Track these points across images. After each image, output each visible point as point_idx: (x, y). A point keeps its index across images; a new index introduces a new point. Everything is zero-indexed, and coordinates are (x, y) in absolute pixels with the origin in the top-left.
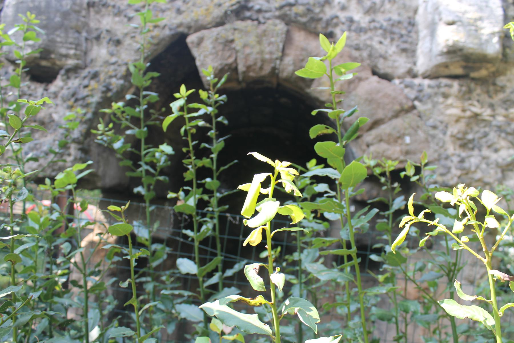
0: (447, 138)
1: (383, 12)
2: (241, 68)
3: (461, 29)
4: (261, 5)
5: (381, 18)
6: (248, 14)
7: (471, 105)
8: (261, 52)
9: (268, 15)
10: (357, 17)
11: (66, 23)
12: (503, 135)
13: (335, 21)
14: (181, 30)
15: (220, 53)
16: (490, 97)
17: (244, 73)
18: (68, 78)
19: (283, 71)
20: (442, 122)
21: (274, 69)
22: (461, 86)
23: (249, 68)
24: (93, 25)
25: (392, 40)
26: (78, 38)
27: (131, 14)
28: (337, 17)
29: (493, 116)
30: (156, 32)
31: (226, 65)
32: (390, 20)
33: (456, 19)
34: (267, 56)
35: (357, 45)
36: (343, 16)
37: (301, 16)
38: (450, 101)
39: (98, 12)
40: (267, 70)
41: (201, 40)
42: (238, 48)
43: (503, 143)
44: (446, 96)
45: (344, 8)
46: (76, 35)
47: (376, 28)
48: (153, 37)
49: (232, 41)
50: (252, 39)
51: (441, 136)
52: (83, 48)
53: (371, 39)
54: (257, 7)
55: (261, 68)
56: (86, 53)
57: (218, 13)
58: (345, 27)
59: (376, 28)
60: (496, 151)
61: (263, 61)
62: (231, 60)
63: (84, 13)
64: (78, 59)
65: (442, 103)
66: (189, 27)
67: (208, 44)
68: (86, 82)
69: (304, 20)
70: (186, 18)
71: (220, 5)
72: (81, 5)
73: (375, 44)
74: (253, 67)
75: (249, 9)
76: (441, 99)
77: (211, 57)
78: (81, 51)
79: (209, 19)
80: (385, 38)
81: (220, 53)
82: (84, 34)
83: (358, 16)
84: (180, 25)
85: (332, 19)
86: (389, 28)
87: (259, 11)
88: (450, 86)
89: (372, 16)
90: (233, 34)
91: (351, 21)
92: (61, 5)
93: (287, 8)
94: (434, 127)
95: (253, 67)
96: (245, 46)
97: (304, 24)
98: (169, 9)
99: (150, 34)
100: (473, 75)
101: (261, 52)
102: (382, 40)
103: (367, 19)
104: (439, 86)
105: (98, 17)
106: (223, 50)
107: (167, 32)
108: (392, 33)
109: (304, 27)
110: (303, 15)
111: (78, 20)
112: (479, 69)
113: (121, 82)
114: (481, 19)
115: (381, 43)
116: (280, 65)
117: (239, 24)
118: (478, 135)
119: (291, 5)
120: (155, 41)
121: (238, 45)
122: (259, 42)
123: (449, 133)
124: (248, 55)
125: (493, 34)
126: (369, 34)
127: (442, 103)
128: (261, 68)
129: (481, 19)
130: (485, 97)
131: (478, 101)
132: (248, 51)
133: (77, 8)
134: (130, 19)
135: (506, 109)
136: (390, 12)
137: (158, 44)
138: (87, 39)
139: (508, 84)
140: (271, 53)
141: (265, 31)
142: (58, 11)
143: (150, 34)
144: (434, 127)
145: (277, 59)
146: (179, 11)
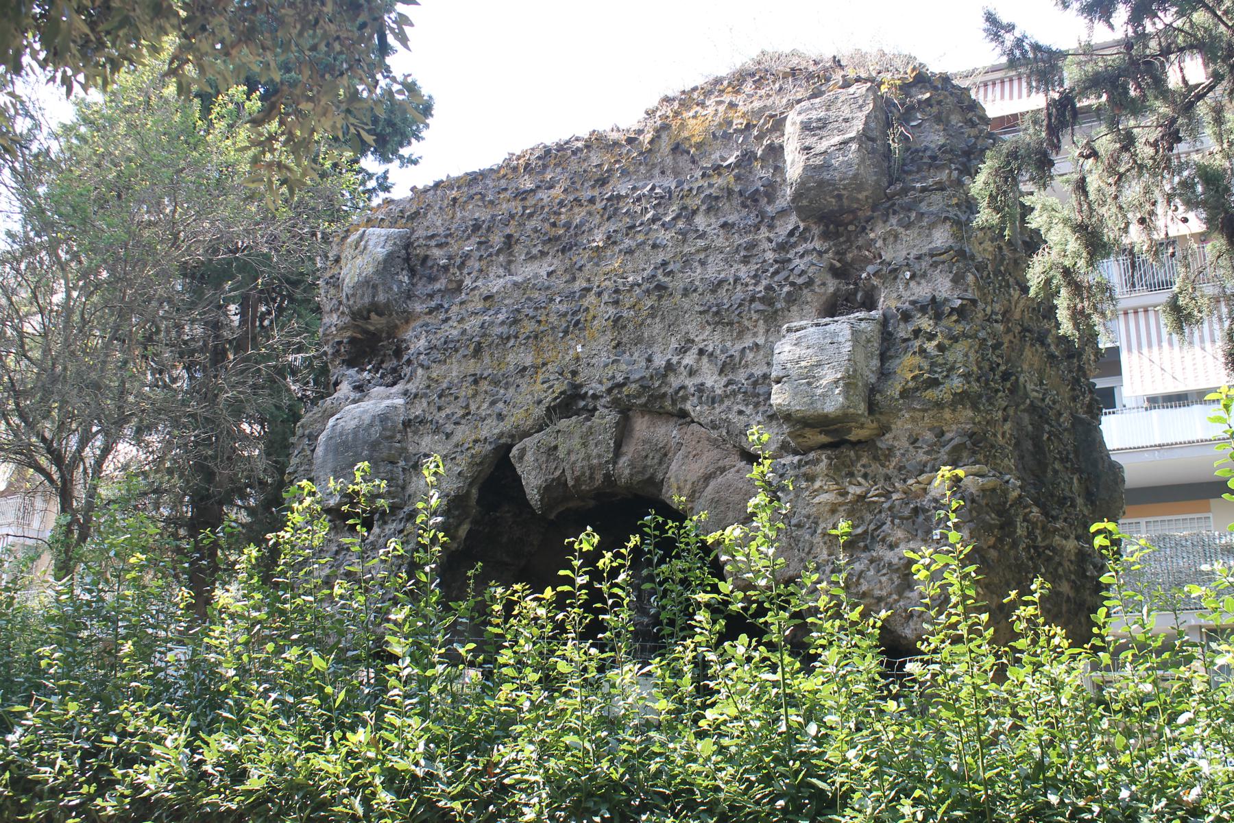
0: (817, 539)
1: (746, 366)
2: (571, 483)
3: (786, 386)
4: (595, 389)
5: (741, 376)
6: (582, 404)
7: (850, 483)
8: (588, 457)
9: (603, 401)
10: (709, 383)
11: (375, 454)
12: (897, 521)
13: (681, 393)
14: (503, 441)
15: (544, 466)
16: (883, 466)
18: (385, 523)
19: (620, 476)
20: (808, 517)
21: (607, 476)
22: (829, 458)
23: (577, 479)
24: (411, 449)
25: (757, 405)
26: (391, 471)
27: (449, 428)
28: (683, 387)
29: (887, 494)
30: (478, 448)
31: (553, 480)
32: (752, 375)
33: (781, 375)
34: (595, 461)
35: (712, 421)
36: (690, 383)
37: (635, 397)
38: (817, 484)
39: (415, 433)
40: (599, 477)
41: (523, 452)
42: (562, 456)
43: (900, 534)
44: (811, 478)
45: (692, 373)
46: (389, 467)
47: (734, 393)
48: (473, 456)
49: (556, 448)
50: (576, 442)
51: (807, 537)
52: (400, 482)
53: (729, 409)
54: (591, 392)
55: (592, 478)
56: (403, 488)
57: (539, 411)
58: (695, 400)
59: (734, 393)
60: (892, 547)
61: (591, 468)
62: (558, 473)
63: (399, 436)
64: (393, 498)
65: (807, 488)
66: (512, 436)
67: (529, 457)
68: (401, 526)
69: (643, 400)
70: (505, 426)
71: (540, 402)
72: (394, 427)
73: (733, 416)
74: (583, 478)
75: (584, 396)
76: (804, 485)
77: (534, 473)
78: (397, 486)
79: (530, 422)
80: (747, 405)
81: (544, 466)
82: (401, 463)
83: (711, 379)
84: (501, 435)
85: (677, 392)
86: (750, 389)
87: (595, 397)
88: (817, 461)
89: (731, 376)
90: (556, 438)
91: (700, 388)
92: (369, 434)
93: (616, 391)
94: (799, 526)
95: (583, 478)
96: (569, 454)
97: (645, 405)
98: (490, 415)
99: (469, 454)
100: (852, 437)
101: (588, 457)
102: (744, 409)
103: (724, 380)
104: (799, 465)
105: (416, 438)
107: (489, 447)
108: (758, 395)
109: (646, 410)
110: (638, 396)
111: (390, 448)
112: (849, 431)
114: (819, 364)
115: (740, 412)
117: (564, 423)
118: (872, 527)
119: (620, 386)
121: (561, 453)
122: (585, 445)
123: (819, 531)
124: (574, 463)
125: (836, 382)
126: (727, 403)
127: (807, 488)
128: (592, 478)
129: (819, 364)
130: (875, 468)
131: (865, 476)
132: (573, 458)
133: (388, 433)
134: (448, 436)
135: (905, 481)
136: (754, 364)
138: (404, 470)
139: (896, 444)
140: (599, 456)
141: (591, 428)
142: (365, 442)
143: (469, 454)
144: (799, 526)
146: (500, 417)
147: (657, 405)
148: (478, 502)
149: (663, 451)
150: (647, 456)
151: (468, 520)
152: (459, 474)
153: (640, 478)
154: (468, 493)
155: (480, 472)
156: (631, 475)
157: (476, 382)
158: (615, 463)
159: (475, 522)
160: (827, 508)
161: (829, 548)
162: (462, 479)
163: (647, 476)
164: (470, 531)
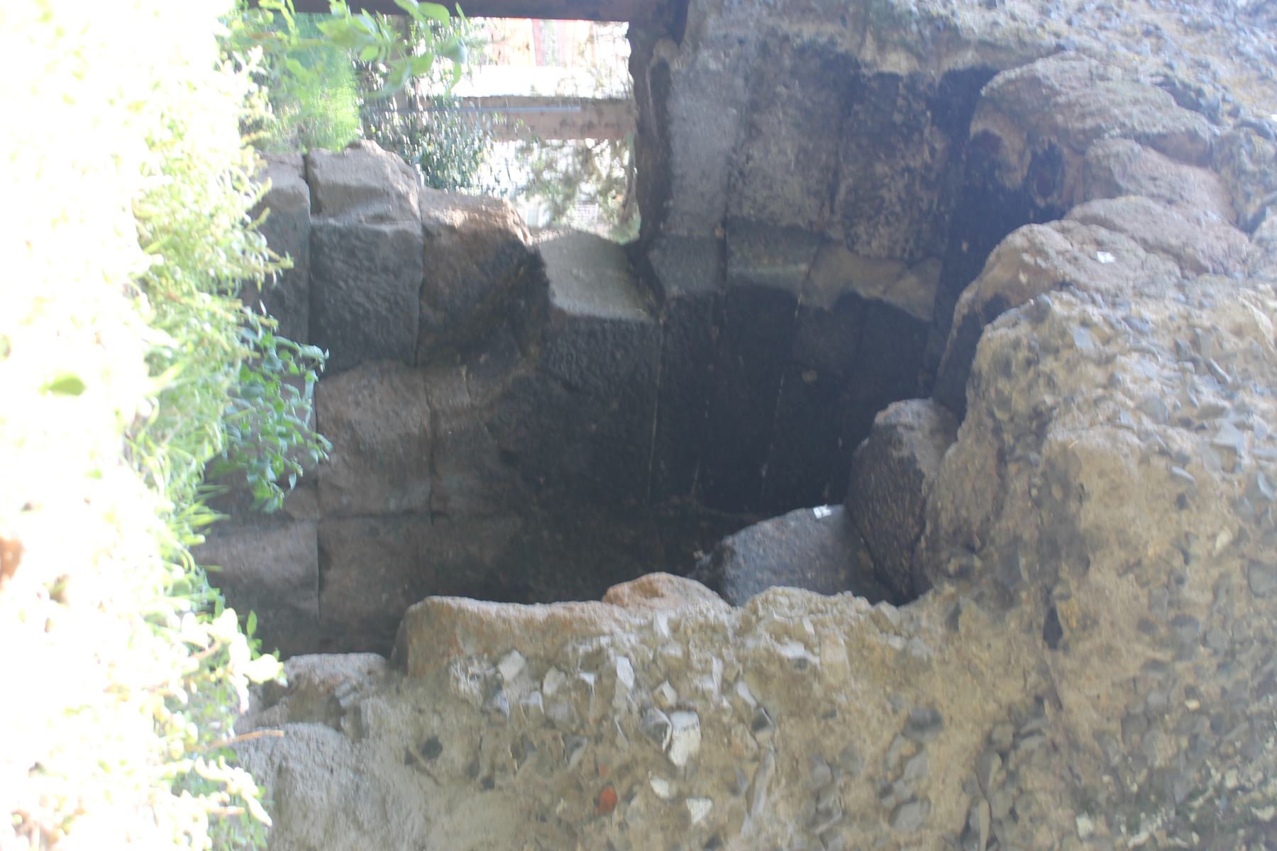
17: (1056, 105)
21: (1097, 132)
37: (1251, 155)
69: (1250, 167)
81: (1067, 75)
93: (1245, 129)
106: (1078, 79)
113: (914, 9)
116: (1112, 137)
120: (1027, 38)
128: (1083, 116)
137: (1022, 44)
145: (1123, 125)
147: (1250, 188)
148: (952, 76)
149: (1177, 198)
150: (1154, 179)
151: (915, 63)
152: (995, 24)
153: (1117, 169)
154: (966, 44)
155: (1007, 49)
156: (1117, 155)
157: (1147, 33)
158: (1125, 136)
159: (913, 77)
160: (1240, 319)
161: (1165, 326)
162: (988, 30)
163: (1123, 183)
164: (894, 77)
